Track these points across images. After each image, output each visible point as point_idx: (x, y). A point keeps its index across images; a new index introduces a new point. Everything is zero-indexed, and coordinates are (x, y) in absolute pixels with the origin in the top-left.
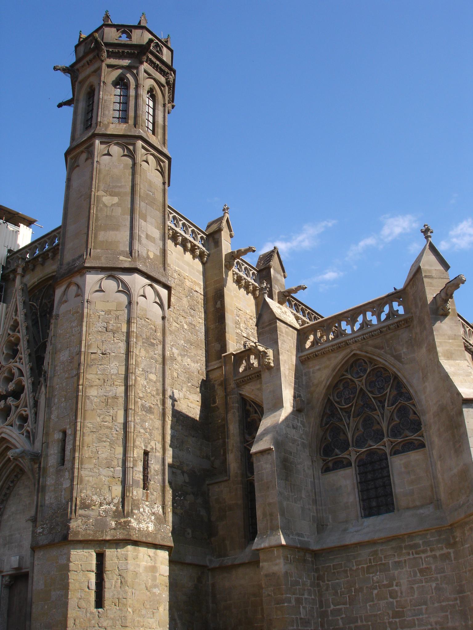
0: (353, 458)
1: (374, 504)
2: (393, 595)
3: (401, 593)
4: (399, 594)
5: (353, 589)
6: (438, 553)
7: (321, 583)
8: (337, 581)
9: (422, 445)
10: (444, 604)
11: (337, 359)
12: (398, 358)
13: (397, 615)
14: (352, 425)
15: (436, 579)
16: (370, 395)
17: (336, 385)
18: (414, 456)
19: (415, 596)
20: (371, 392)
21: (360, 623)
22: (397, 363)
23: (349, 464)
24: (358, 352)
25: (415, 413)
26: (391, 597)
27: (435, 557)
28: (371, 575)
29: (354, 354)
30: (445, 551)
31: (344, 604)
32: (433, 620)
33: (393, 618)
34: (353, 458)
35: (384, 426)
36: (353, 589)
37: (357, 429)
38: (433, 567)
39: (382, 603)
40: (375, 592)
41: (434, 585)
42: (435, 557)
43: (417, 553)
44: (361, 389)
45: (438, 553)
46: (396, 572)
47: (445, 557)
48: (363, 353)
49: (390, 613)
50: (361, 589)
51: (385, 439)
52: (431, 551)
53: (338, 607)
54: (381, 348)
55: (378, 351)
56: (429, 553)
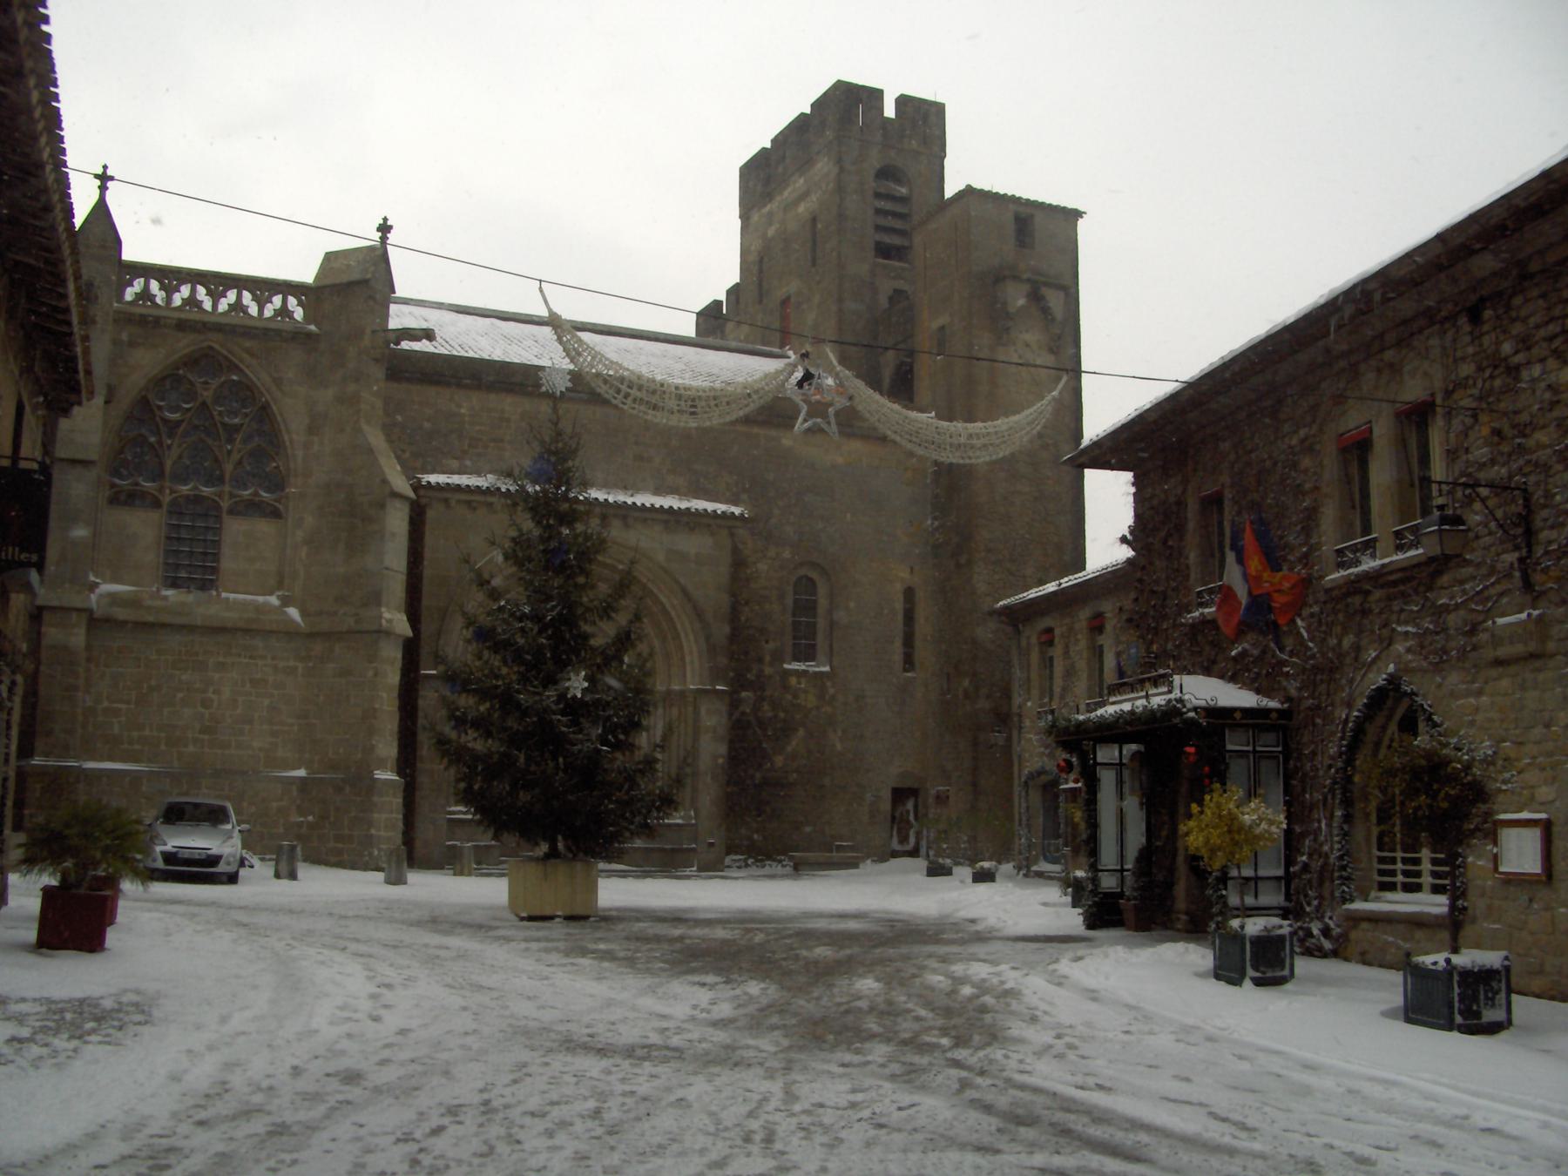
0: (166, 499)
2: (206, 704)
4: (215, 704)
5: (145, 686)
6: (281, 664)
8: (120, 670)
9: (276, 514)
10: (275, 728)
11: (185, 344)
12: (278, 382)
13: (204, 730)
14: (175, 452)
17: (164, 379)
18: (264, 527)
19: (239, 711)
24: (217, 346)
27: (275, 667)
28: (178, 672)
29: (211, 348)
30: (291, 663)
31: (128, 702)
32: (256, 744)
33: (200, 733)
34: (166, 499)
36: (145, 686)
40: (180, 695)
41: (267, 702)
42: (275, 667)
43: (251, 657)
45: (281, 664)
46: (217, 676)
48: (225, 353)
51: (227, 488)
52: (274, 658)
53: (115, 705)
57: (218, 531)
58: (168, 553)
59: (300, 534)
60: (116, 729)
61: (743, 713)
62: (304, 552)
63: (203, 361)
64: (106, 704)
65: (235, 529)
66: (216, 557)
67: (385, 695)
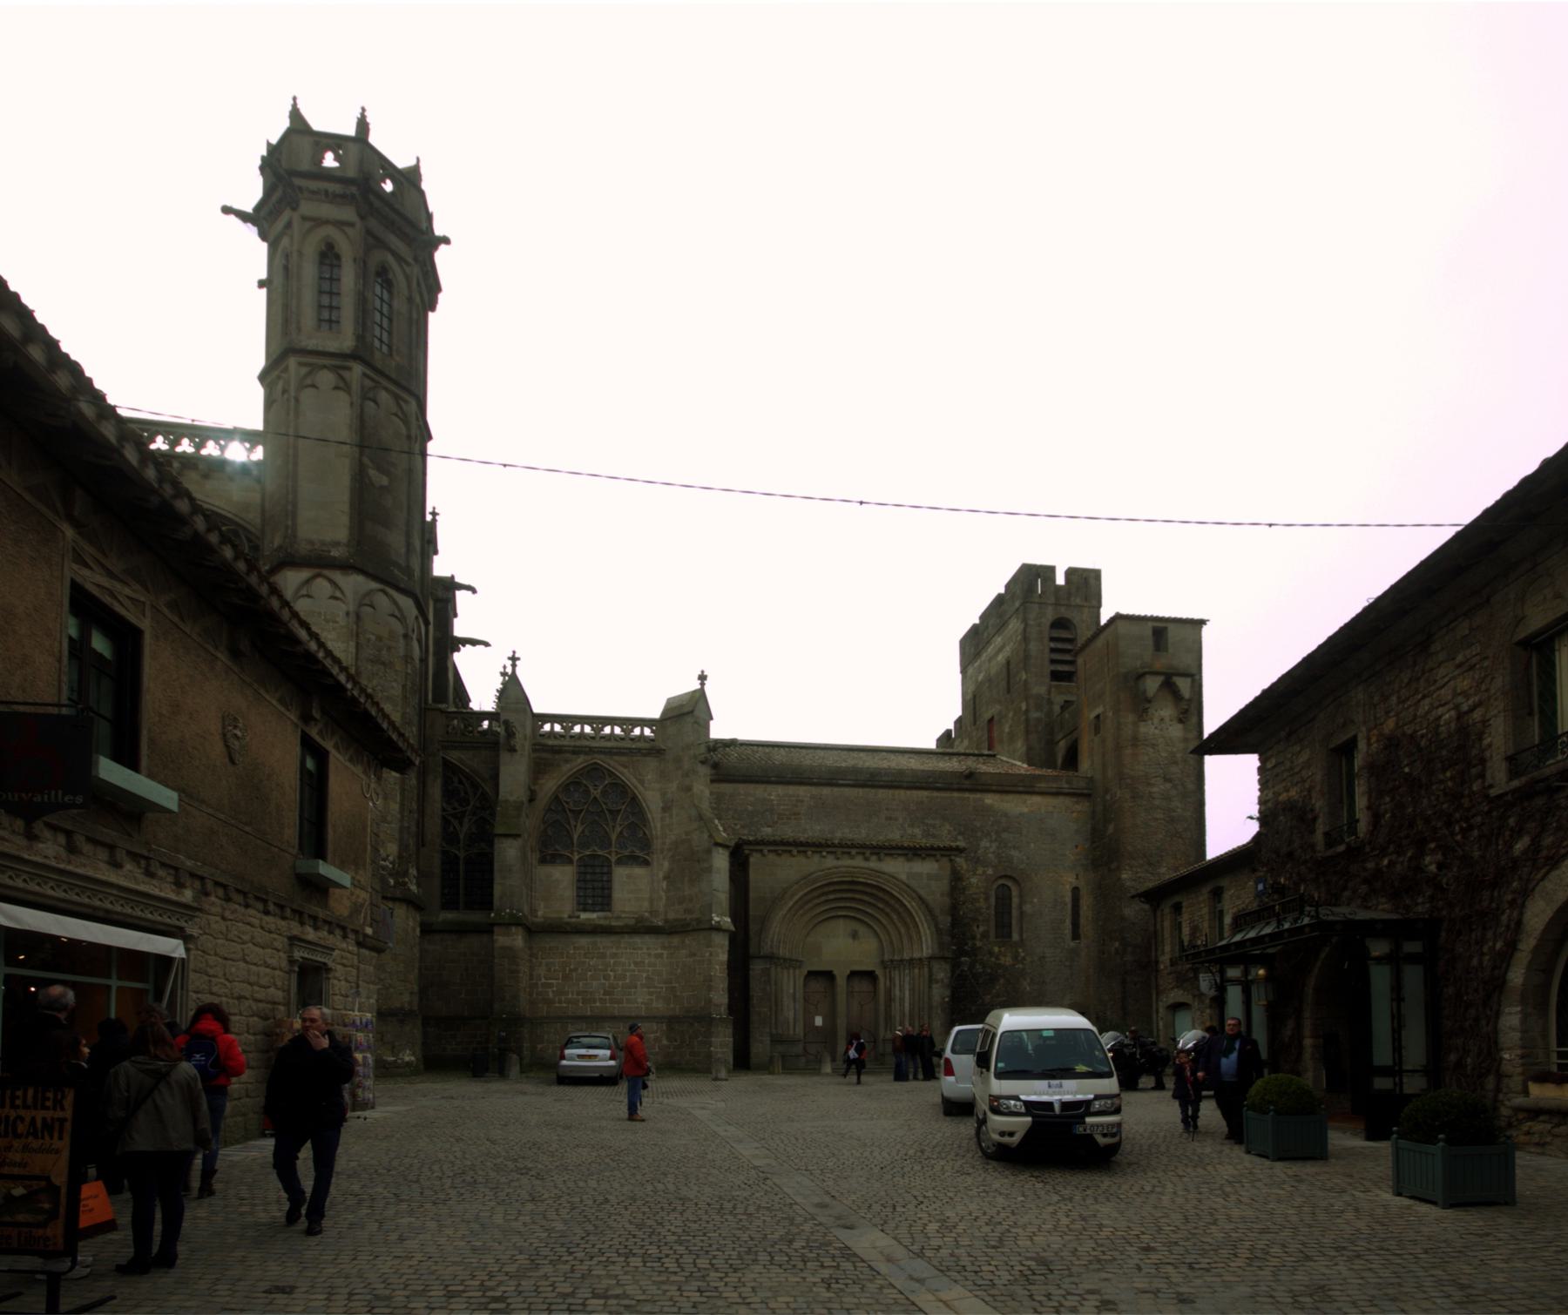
0: (576, 857)
1: (590, 902)
2: (606, 978)
3: (615, 977)
6: (653, 952)
7: (534, 960)
9: (646, 863)
12: (642, 782)
15: (648, 971)
16: (604, 806)
18: (639, 871)
20: (605, 804)
21: (570, 996)
22: (639, 786)
23: (570, 861)
25: (645, 833)
26: (605, 978)
27: (649, 955)
30: (659, 951)
35: (614, 837)
37: (583, 832)
38: (647, 961)
39: (595, 983)
41: (644, 975)
42: (649, 955)
44: (595, 798)
47: (660, 956)
49: (602, 992)
50: (575, 970)
51: (613, 849)
54: (625, 767)
55: (621, 769)
56: (645, 951)
57: (610, 873)
58: (578, 888)
59: (661, 875)
60: (551, 995)
61: (963, 971)
62: (664, 884)
63: (594, 771)
64: (543, 980)
65: (620, 874)
66: (610, 889)
67: (717, 967)
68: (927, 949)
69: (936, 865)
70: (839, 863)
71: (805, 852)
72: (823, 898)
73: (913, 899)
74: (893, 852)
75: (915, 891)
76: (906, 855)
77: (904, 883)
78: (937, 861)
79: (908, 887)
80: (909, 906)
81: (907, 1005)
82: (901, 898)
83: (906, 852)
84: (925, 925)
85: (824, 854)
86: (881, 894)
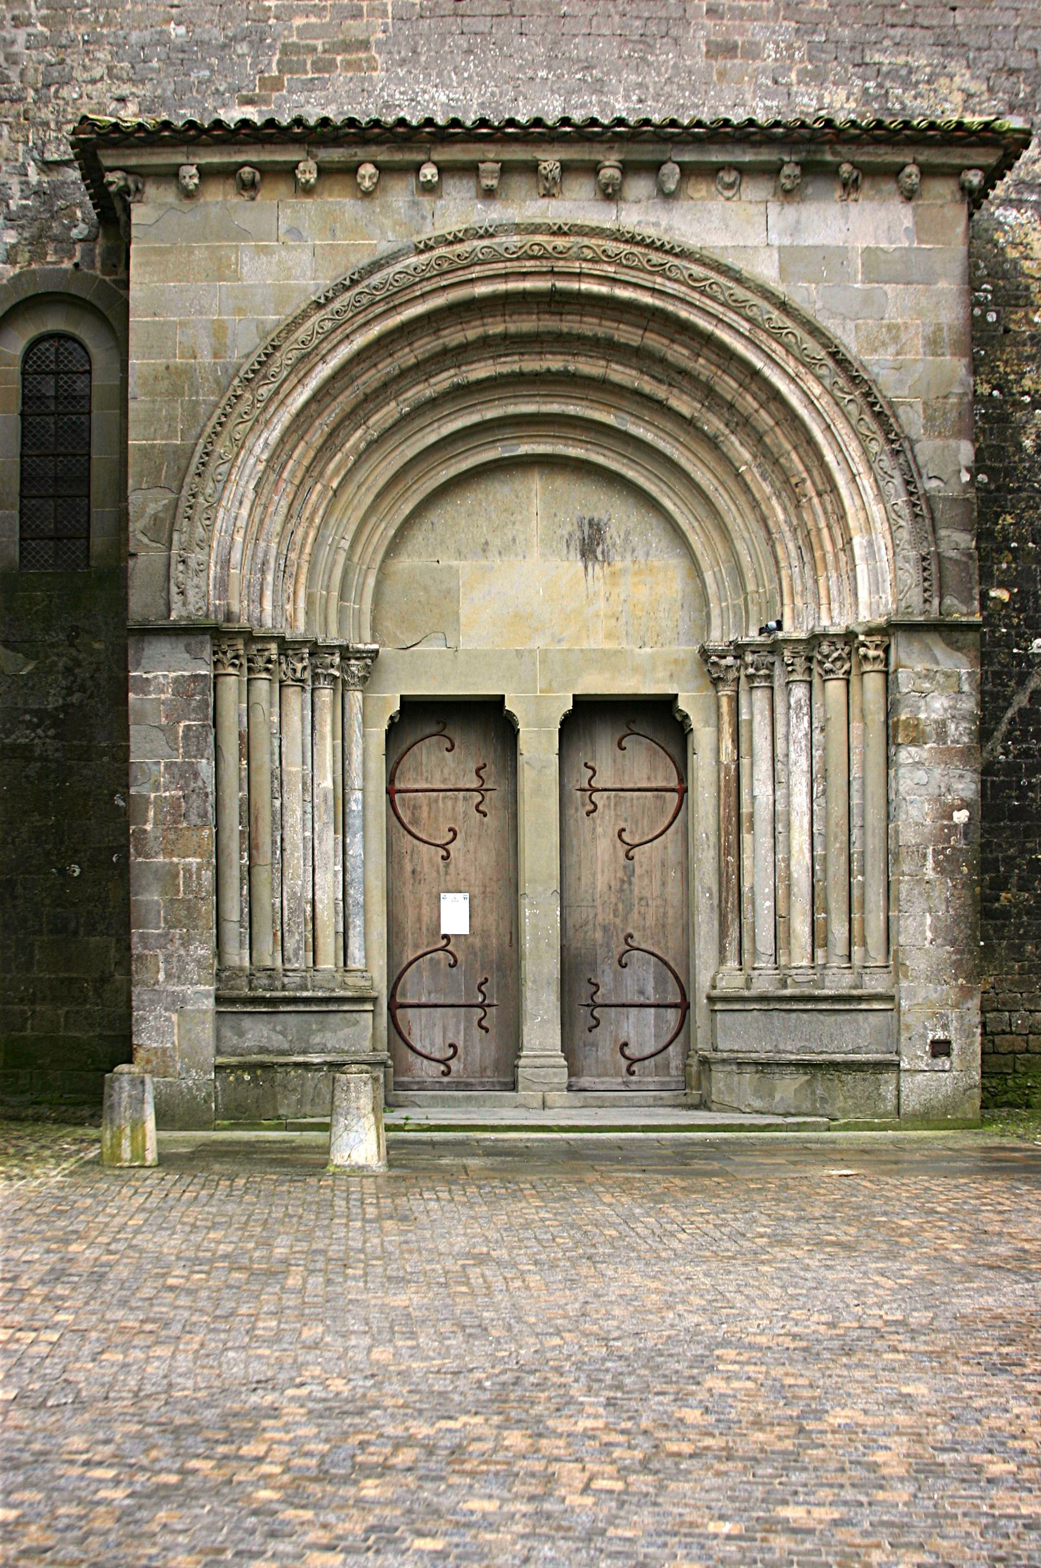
68: (876, 587)
69: (903, 215)
70: (495, 213)
71: (351, 170)
72: (444, 380)
73: (809, 364)
74: (716, 156)
75: (814, 331)
76: (772, 171)
77: (767, 294)
78: (909, 196)
79: (783, 306)
80: (795, 400)
81: (800, 840)
82: (758, 363)
83: (765, 155)
84: (866, 482)
85: (429, 172)
86: (678, 353)
